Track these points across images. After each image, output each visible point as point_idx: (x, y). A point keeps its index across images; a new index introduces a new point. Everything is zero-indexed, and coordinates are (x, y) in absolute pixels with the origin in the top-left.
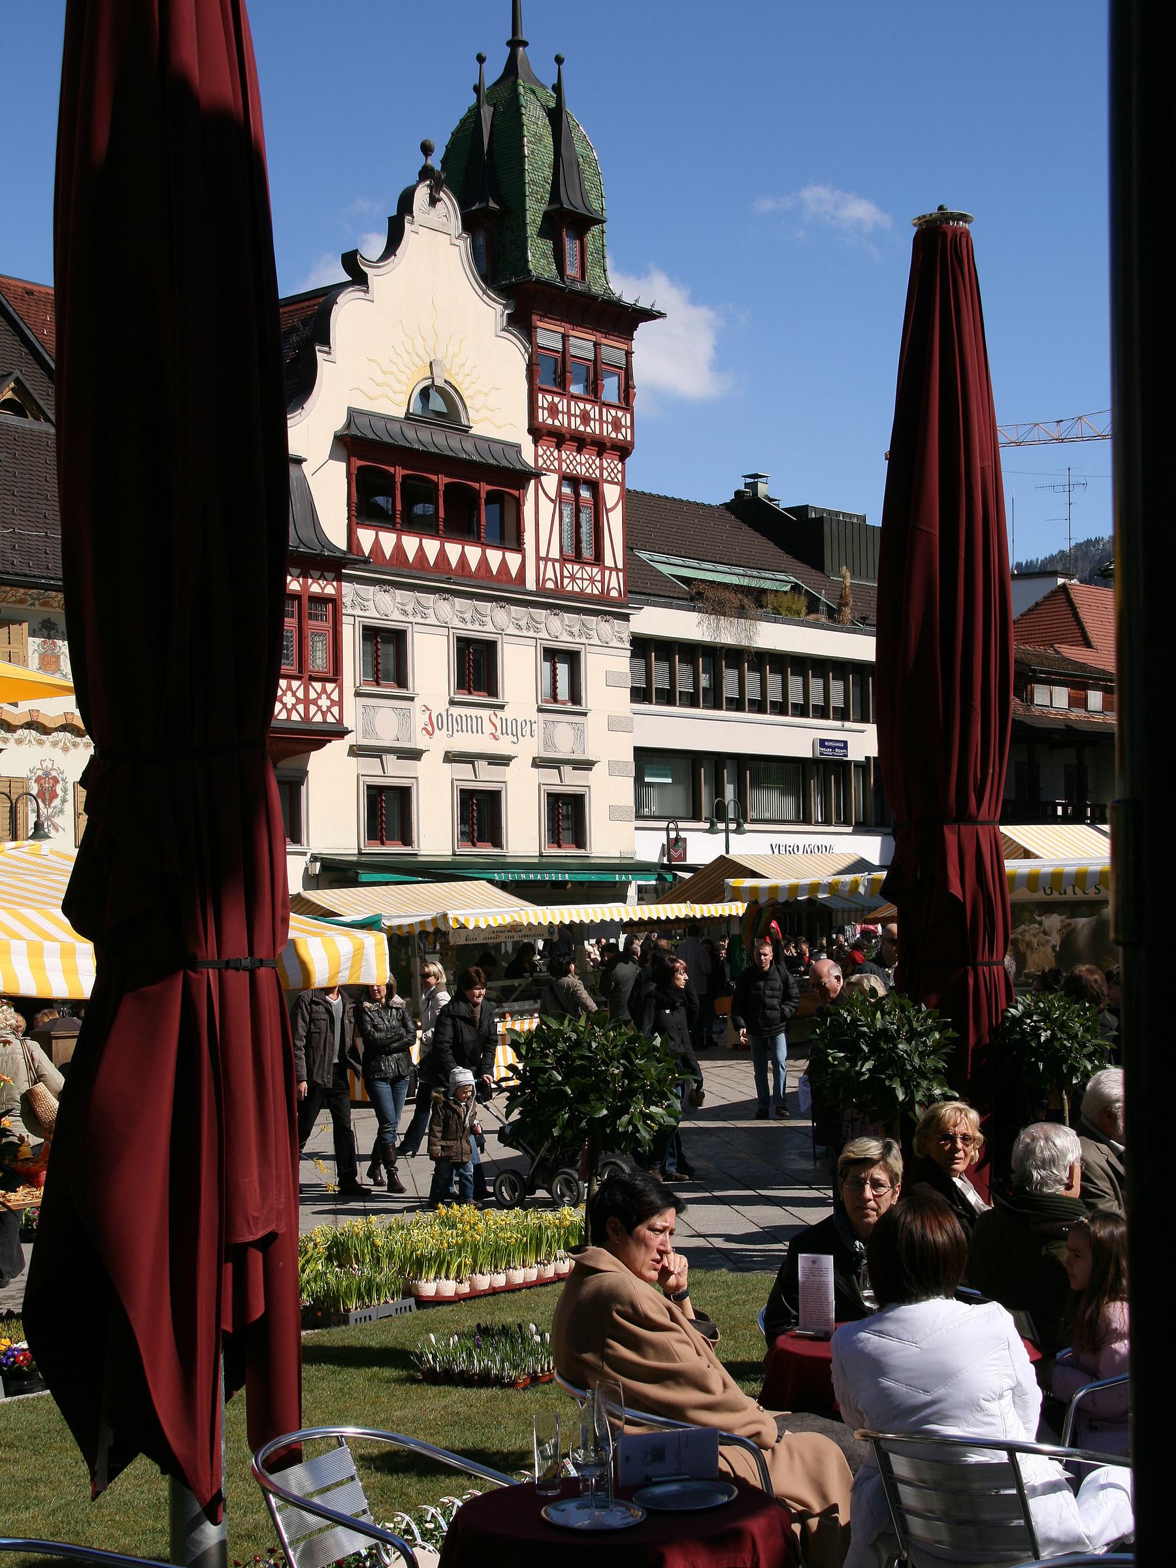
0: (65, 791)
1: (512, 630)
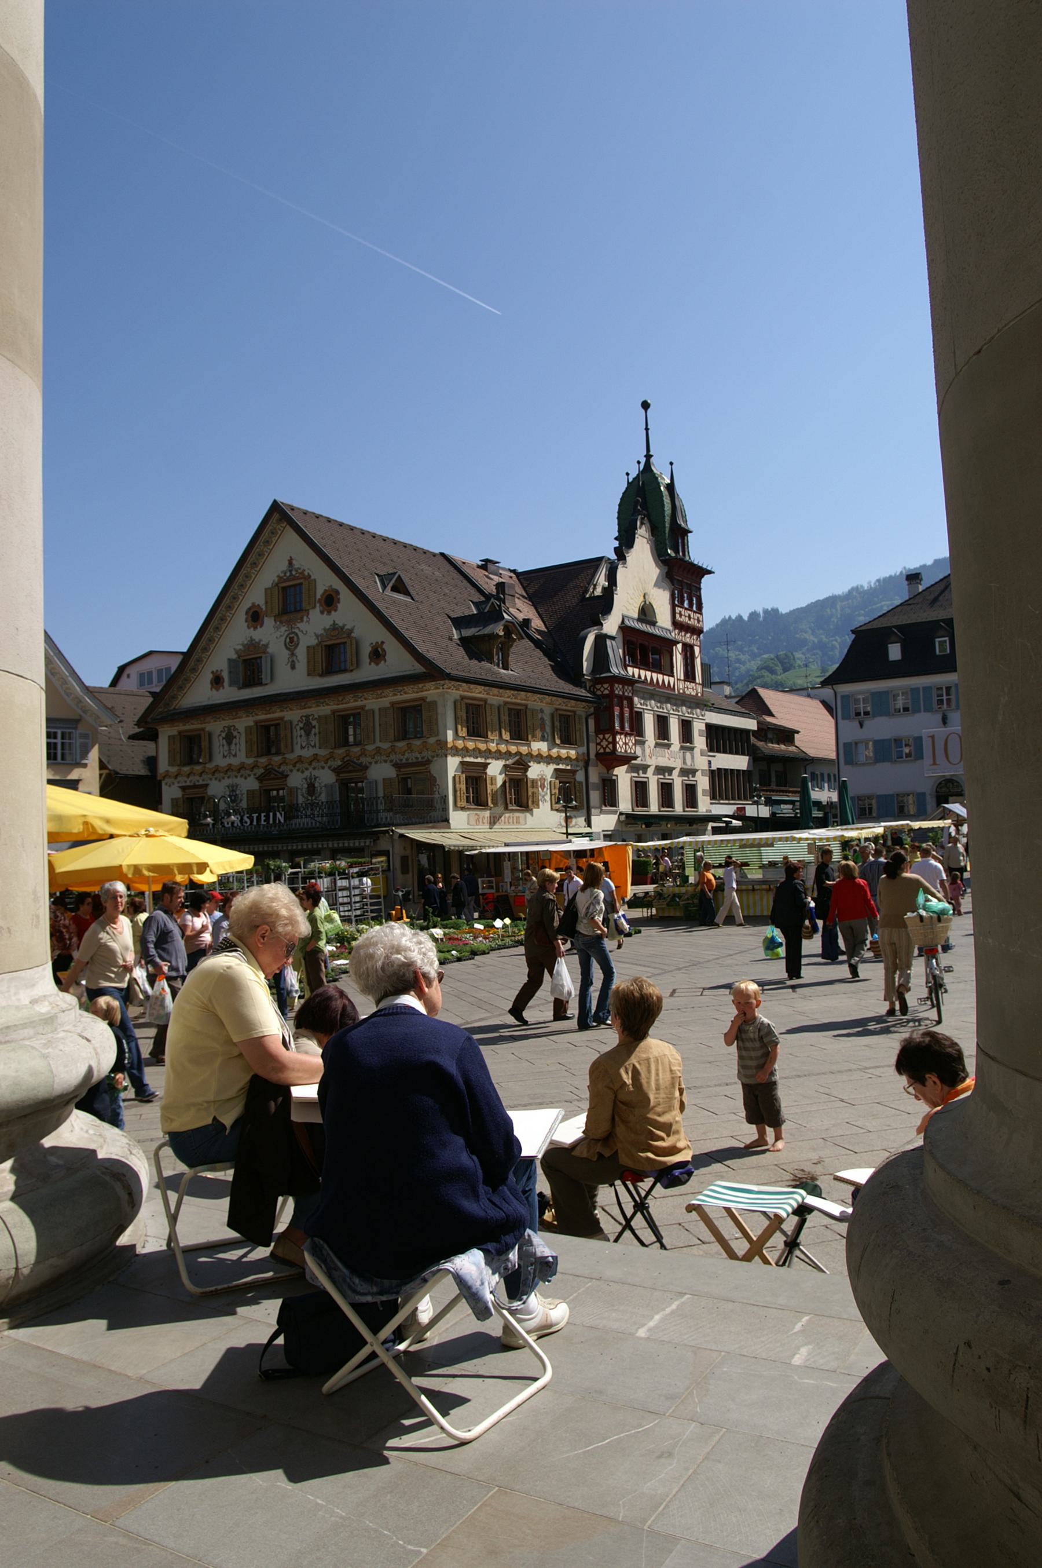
1: (672, 712)
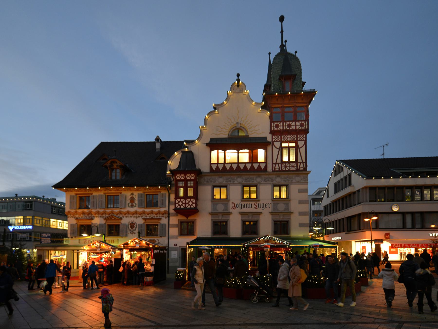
0: (136, 226)
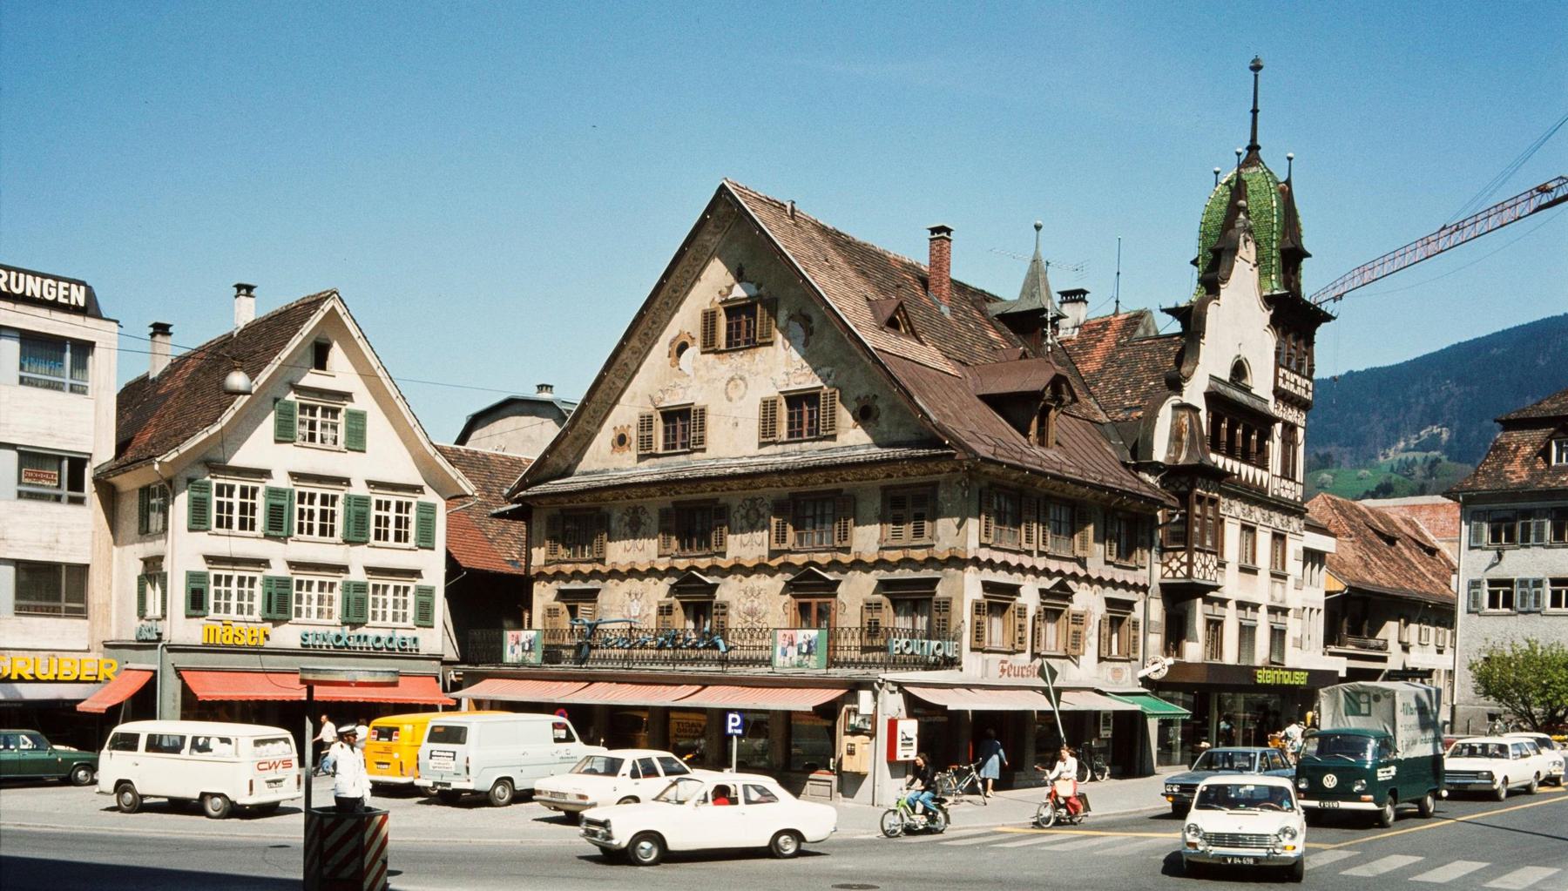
1: (1262, 522)
